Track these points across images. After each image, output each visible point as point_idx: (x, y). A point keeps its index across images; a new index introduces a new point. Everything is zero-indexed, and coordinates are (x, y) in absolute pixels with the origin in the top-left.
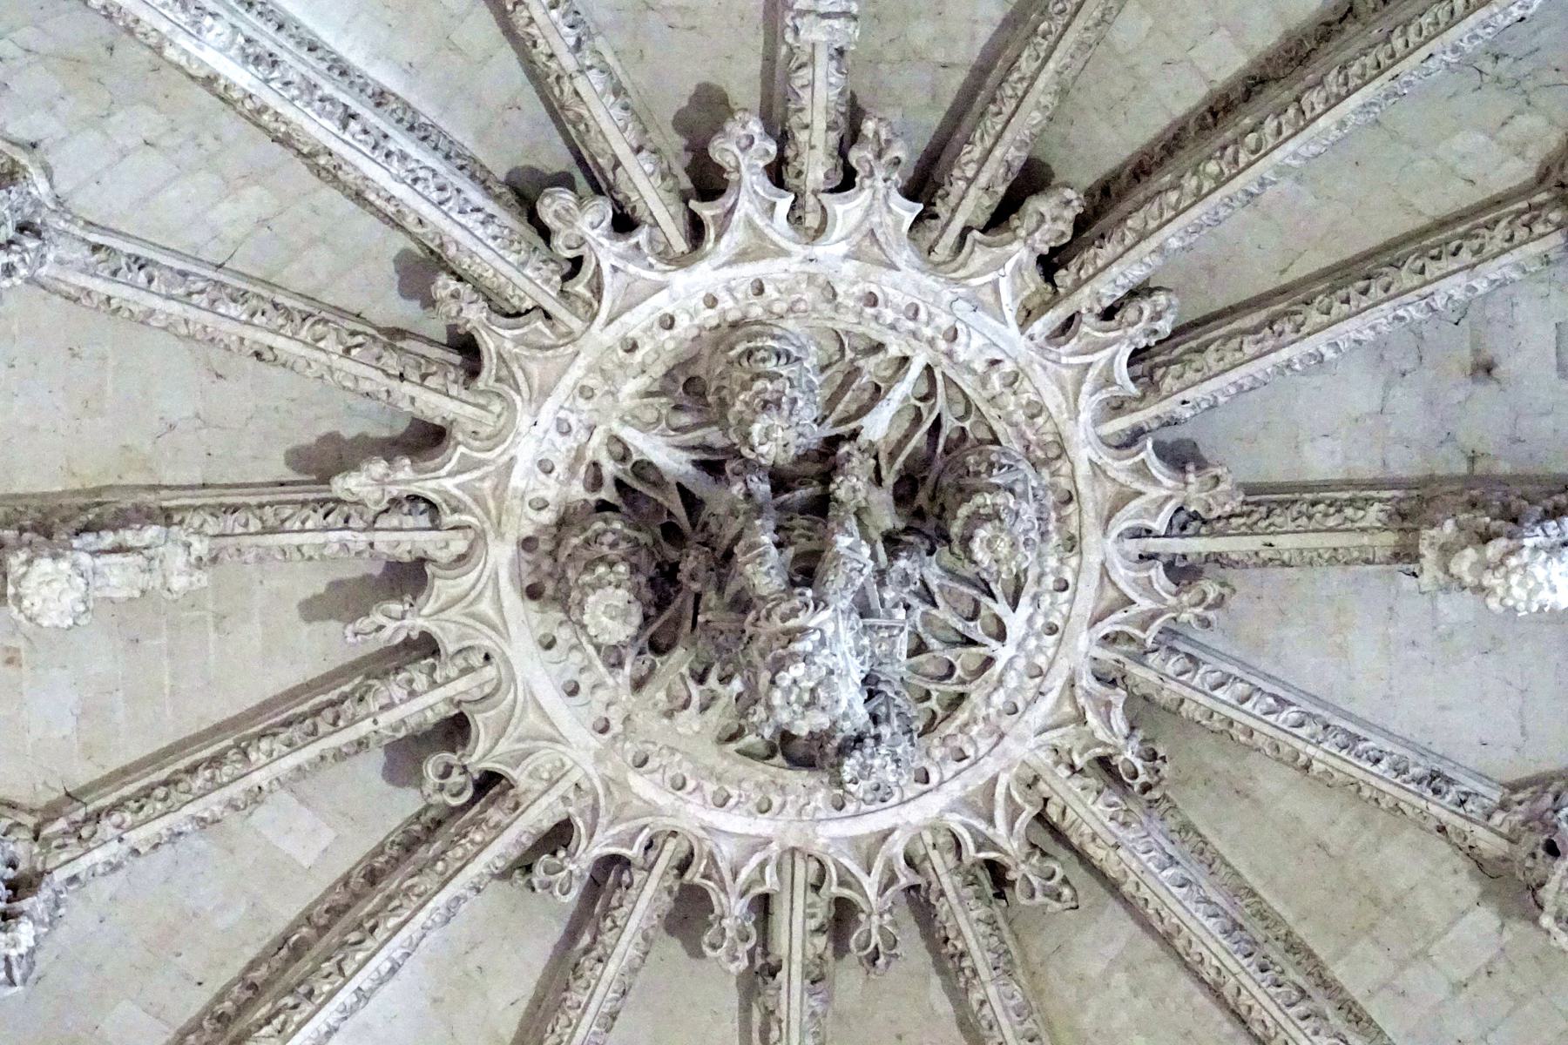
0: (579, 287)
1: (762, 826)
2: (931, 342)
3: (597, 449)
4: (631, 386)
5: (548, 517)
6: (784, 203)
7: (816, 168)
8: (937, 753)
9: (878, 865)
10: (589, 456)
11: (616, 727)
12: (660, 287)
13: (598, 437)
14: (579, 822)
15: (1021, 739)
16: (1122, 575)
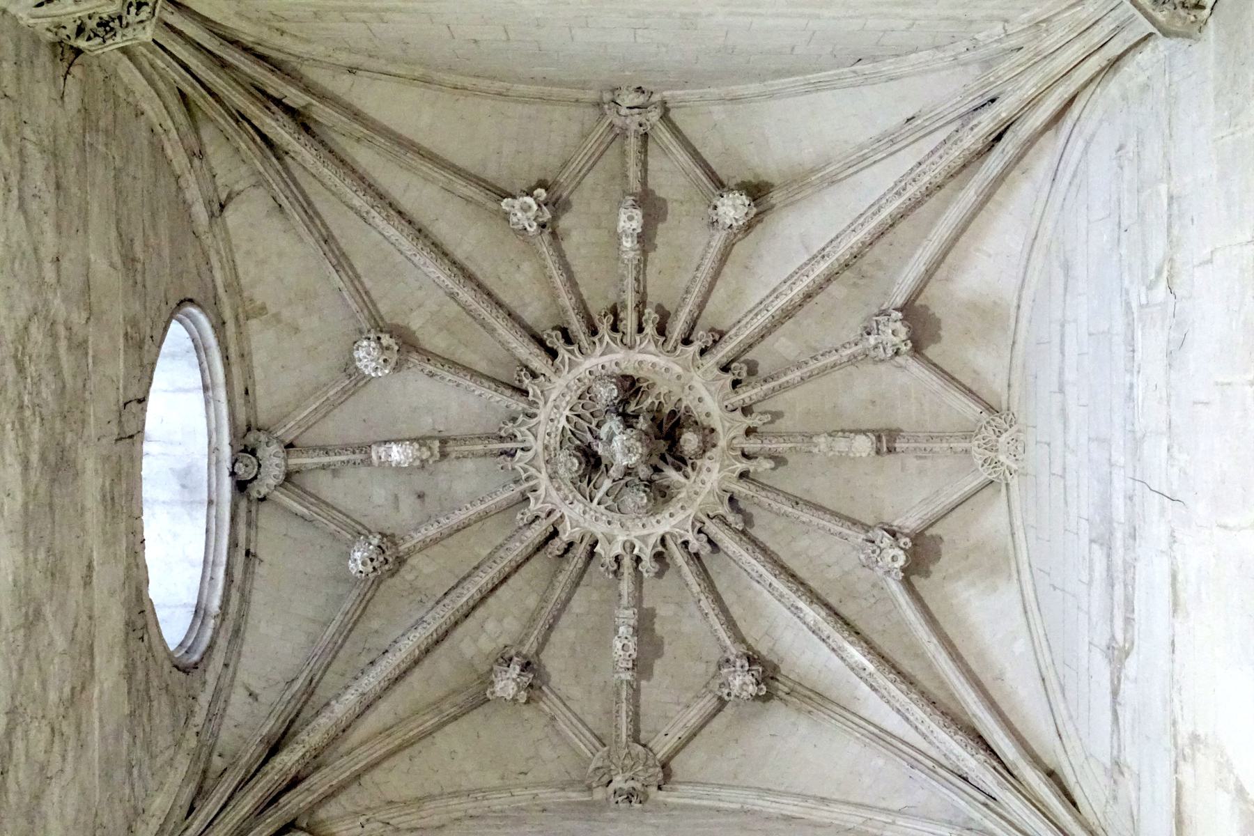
0: (698, 525)
1: (640, 357)
2: (591, 509)
3: (693, 475)
4: (682, 495)
5: (708, 454)
6: (636, 551)
7: (627, 562)
8: (586, 381)
9: (605, 344)
10: (695, 473)
11: (687, 387)
12: (674, 526)
13: (692, 479)
14: (698, 357)
15: (561, 385)
16: (531, 438)
